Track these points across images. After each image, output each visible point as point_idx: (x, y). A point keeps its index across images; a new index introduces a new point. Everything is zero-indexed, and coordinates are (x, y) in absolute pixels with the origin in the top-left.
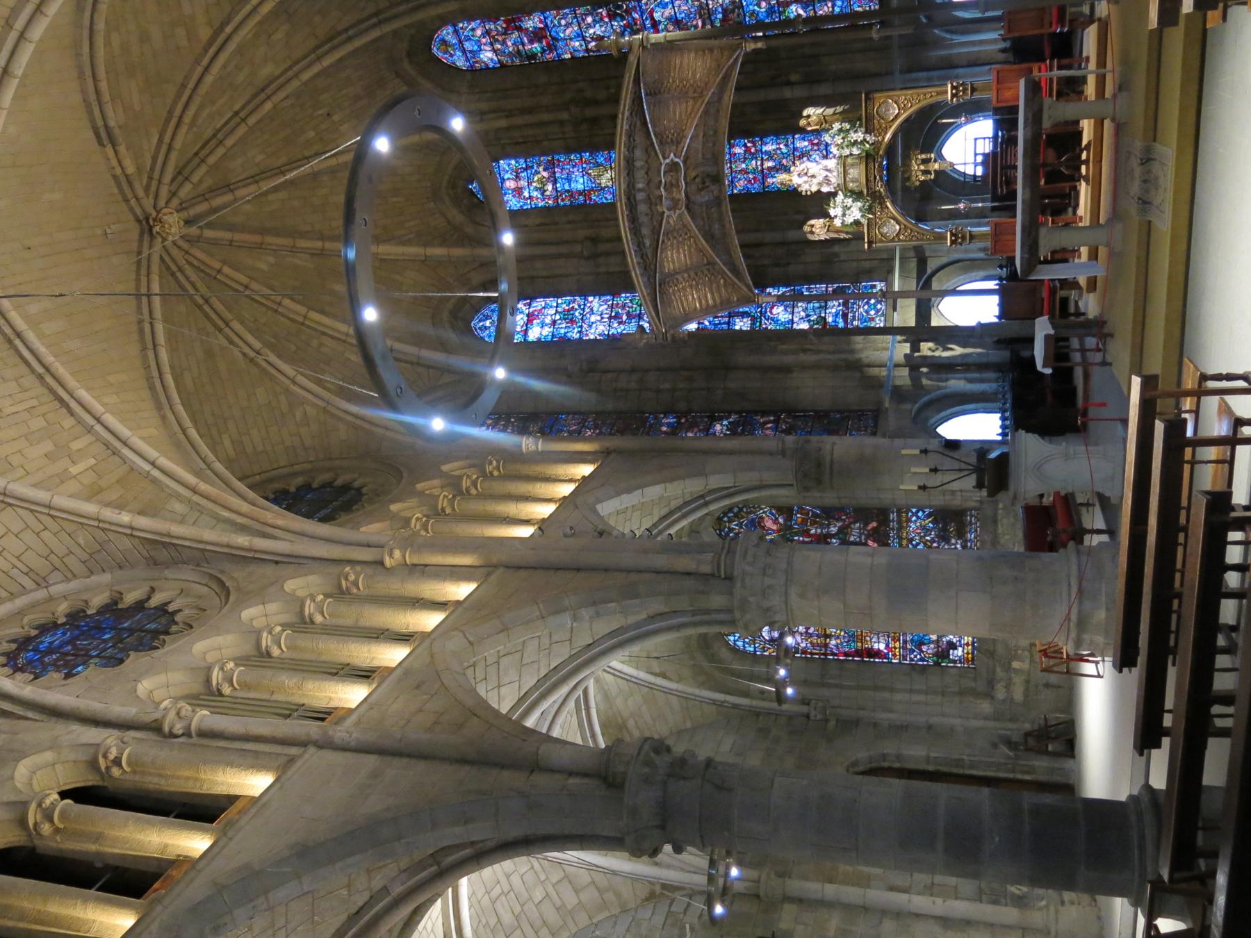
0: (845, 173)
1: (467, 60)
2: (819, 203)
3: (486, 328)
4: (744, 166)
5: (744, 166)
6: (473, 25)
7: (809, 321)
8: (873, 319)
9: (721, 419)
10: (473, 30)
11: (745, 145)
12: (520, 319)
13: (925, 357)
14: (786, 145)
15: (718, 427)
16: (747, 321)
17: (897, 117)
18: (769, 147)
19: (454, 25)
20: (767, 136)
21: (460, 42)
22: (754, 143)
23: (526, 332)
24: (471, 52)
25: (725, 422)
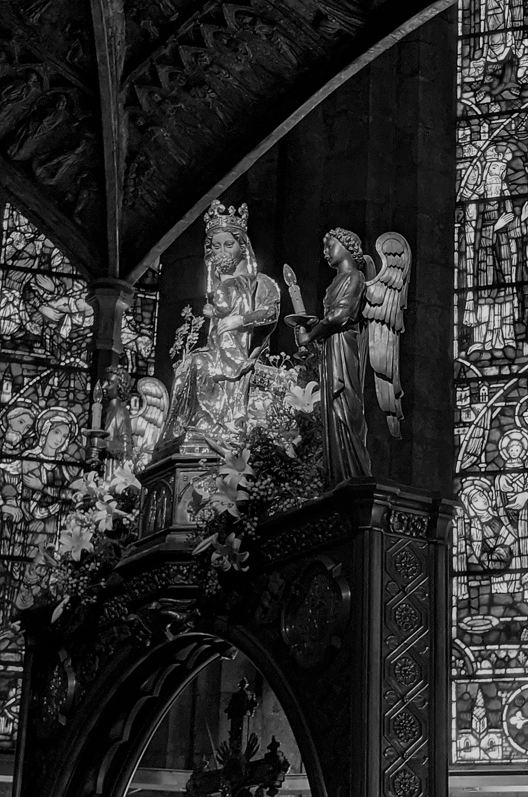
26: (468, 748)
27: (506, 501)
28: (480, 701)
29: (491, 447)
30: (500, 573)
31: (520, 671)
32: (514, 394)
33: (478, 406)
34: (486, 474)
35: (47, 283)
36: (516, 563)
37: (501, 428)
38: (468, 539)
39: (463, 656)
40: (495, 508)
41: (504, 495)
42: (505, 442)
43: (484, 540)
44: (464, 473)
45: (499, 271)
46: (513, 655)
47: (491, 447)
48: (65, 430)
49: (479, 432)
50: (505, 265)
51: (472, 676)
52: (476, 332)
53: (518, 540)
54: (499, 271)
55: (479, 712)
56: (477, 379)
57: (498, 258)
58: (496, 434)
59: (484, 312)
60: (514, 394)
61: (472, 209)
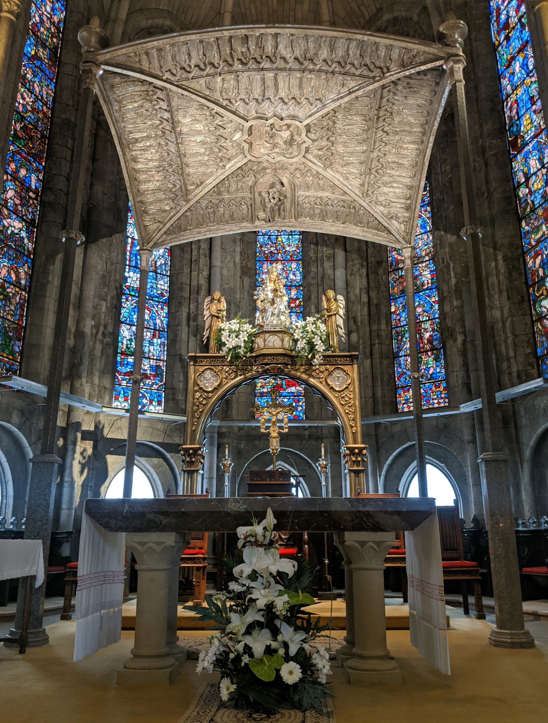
11: (297, 299)
13: (75, 443)
22: (299, 306)
25: (23, 234)
28: (122, 392)
33: (128, 303)
34: (129, 324)
35: (6, 212)
38: (122, 343)
39: (118, 378)
43: (127, 345)
44: (123, 323)
45: (136, 263)
48: (7, 269)
49: (128, 311)
51: (120, 385)
54: (136, 263)
55: (122, 396)
59: (131, 274)
61: (130, 240)
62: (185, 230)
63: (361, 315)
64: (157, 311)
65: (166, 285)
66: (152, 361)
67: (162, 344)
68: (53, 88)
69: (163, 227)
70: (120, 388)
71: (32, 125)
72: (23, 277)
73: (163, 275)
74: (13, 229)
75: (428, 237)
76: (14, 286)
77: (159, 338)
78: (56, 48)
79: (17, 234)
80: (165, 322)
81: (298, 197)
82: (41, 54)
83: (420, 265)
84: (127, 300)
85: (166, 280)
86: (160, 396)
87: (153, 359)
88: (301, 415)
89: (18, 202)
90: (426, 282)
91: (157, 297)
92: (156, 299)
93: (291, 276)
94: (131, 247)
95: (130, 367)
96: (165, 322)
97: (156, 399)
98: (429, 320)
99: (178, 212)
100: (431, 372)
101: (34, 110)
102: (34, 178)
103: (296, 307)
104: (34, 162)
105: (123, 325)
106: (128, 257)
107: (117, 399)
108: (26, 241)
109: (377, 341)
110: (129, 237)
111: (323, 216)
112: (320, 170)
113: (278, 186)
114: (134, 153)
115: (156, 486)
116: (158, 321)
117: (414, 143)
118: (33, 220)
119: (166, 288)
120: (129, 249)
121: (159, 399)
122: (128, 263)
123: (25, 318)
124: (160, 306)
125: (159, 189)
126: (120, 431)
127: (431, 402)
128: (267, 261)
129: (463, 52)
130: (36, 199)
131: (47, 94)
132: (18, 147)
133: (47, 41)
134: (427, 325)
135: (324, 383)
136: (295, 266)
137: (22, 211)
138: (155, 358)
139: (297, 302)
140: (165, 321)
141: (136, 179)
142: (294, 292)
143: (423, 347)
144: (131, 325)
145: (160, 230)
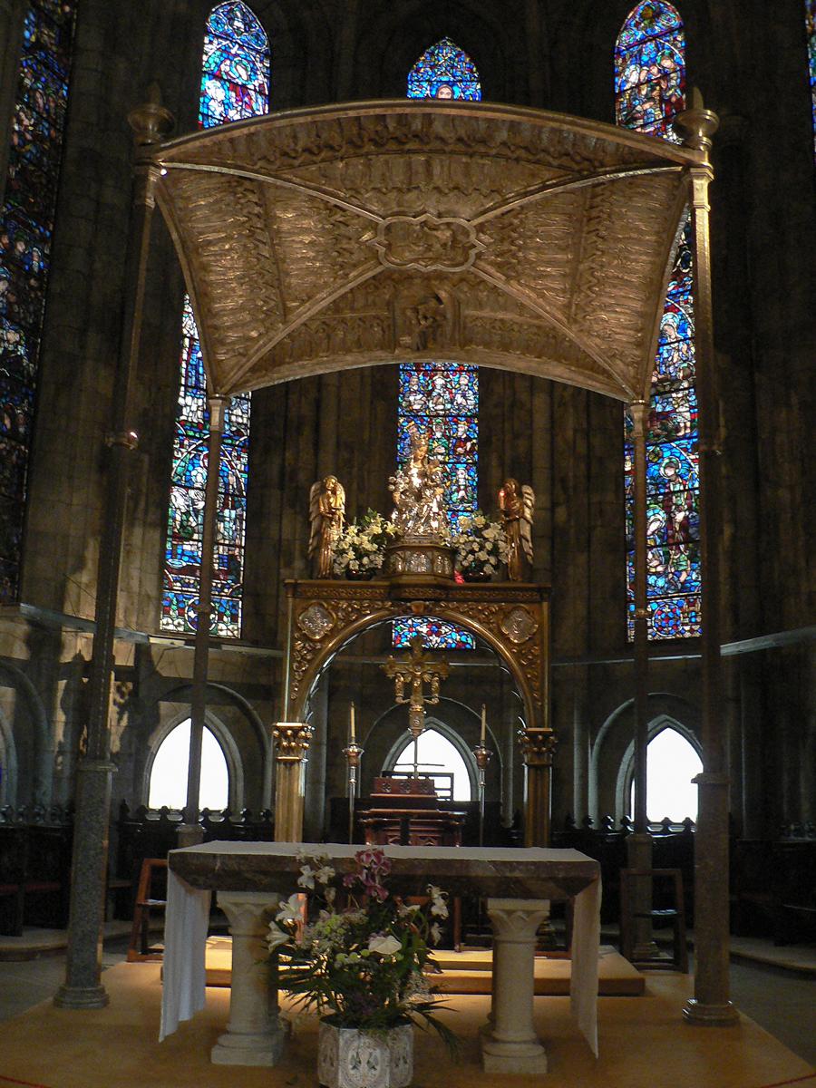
0: (421, 549)
1: (629, 47)
2: (372, 497)
3: (231, 20)
4: (438, 435)
5: (438, 435)
6: (679, 55)
7: (187, 513)
8: (181, 614)
9: (30, 346)
10: (672, 55)
11: (468, 439)
12: (240, 74)
14: (462, 500)
15: (13, 336)
16: (198, 417)
17: (505, 639)
18: (461, 474)
19: (680, 29)
20: (478, 472)
21: (655, 37)
22: (471, 452)
23: (216, 76)
24: (640, 52)
25: (21, 351)
26: (168, 624)
27: (193, 504)
28: (175, 602)
29: (188, 474)
30: (188, 540)
31: (194, 590)
32: (201, 449)
33: (183, 450)
36: (196, 536)
37: (193, 465)
38: (174, 519)
40: (188, 506)
41: (192, 499)
42: (194, 473)
44: (175, 484)
45: (197, 379)
46: (192, 582)
47: (188, 474)
49: (183, 464)
50: (201, 377)
51: (171, 589)
52: (184, 410)
53: (198, 525)
54: (197, 379)
56: (182, 435)
57: (197, 372)
58: (191, 468)
59: (189, 400)
60: (201, 449)
61: (187, 341)
62: (282, 363)
63: (575, 476)
64: (229, 462)
65: (245, 416)
66: (221, 548)
67: (239, 517)
68: (65, 93)
69: (248, 361)
70: (171, 595)
71: (34, 165)
72: (21, 422)
73: (241, 398)
74: (6, 344)
75: (689, 349)
76: (9, 438)
77: (234, 508)
78: (69, 22)
79: (13, 352)
80: (243, 480)
81: (466, 317)
82: (46, 38)
83: (674, 395)
84: (182, 445)
85: (245, 407)
86: (235, 607)
87: (223, 545)
88: (470, 641)
89: (13, 299)
90: (682, 425)
91: (230, 437)
92: (230, 441)
93: (459, 399)
94: (189, 354)
95: (186, 559)
96: (243, 480)
97: (228, 612)
98: (685, 490)
99: (270, 341)
100: (682, 579)
101: (38, 138)
102: (36, 253)
103: (467, 453)
104: (37, 227)
105: (175, 489)
106: (183, 371)
107: (167, 613)
108: (25, 361)
109: (599, 523)
110: (185, 336)
111: (506, 347)
112: (500, 285)
113: (433, 303)
114: (205, 259)
115: (231, 753)
116: (232, 479)
117: (647, 254)
118: (36, 323)
119: (245, 421)
120: (185, 356)
121: (234, 611)
122: (183, 382)
123: (25, 488)
124: (234, 454)
125: (242, 308)
126: (173, 666)
127: (680, 628)
128: (418, 371)
129: (710, 161)
130: (40, 288)
131: (56, 106)
132: (13, 206)
133: (54, 12)
134: (681, 500)
135: (495, 631)
136: (466, 381)
137: (19, 313)
138: (227, 542)
139: (469, 445)
140: (243, 478)
141: (206, 294)
142: (462, 429)
143: (673, 536)
144: (187, 488)
145: (242, 366)
